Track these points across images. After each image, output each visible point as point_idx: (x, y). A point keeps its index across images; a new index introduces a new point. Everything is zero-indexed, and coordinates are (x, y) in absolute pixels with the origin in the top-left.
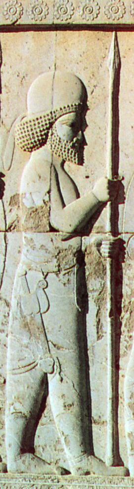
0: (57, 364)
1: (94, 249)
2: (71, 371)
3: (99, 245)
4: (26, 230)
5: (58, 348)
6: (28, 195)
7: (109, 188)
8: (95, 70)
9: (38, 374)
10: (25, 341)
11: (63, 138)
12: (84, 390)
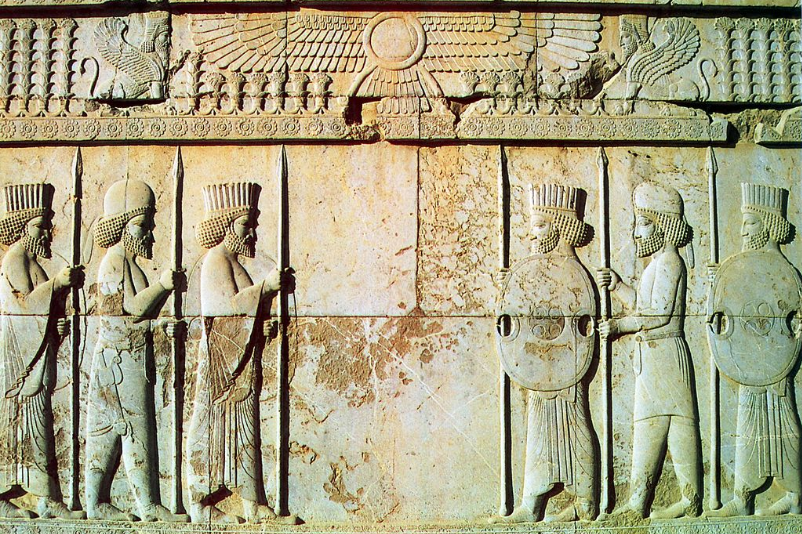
0: (129, 427)
1: (161, 330)
2: (141, 433)
3: (165, 326)
4: (103, 314)
5: (131, 414)
6: (105, 284)
7: (173, 278)
8: (162, 178)
9: (113, 435)
10: (103, 408)
11: (134, 236)
12: (152, 449)
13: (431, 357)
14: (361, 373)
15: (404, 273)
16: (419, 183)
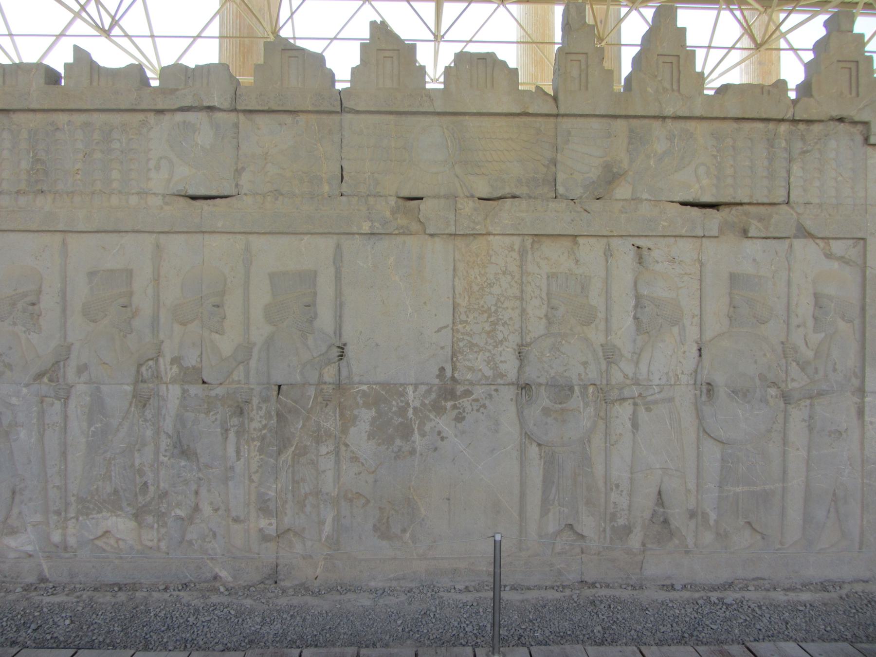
13: (464, 418)
14: (406, 432)
15: (442, 348)
16: (454, 270)
